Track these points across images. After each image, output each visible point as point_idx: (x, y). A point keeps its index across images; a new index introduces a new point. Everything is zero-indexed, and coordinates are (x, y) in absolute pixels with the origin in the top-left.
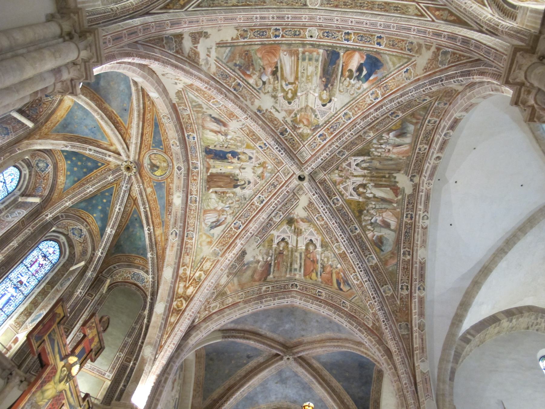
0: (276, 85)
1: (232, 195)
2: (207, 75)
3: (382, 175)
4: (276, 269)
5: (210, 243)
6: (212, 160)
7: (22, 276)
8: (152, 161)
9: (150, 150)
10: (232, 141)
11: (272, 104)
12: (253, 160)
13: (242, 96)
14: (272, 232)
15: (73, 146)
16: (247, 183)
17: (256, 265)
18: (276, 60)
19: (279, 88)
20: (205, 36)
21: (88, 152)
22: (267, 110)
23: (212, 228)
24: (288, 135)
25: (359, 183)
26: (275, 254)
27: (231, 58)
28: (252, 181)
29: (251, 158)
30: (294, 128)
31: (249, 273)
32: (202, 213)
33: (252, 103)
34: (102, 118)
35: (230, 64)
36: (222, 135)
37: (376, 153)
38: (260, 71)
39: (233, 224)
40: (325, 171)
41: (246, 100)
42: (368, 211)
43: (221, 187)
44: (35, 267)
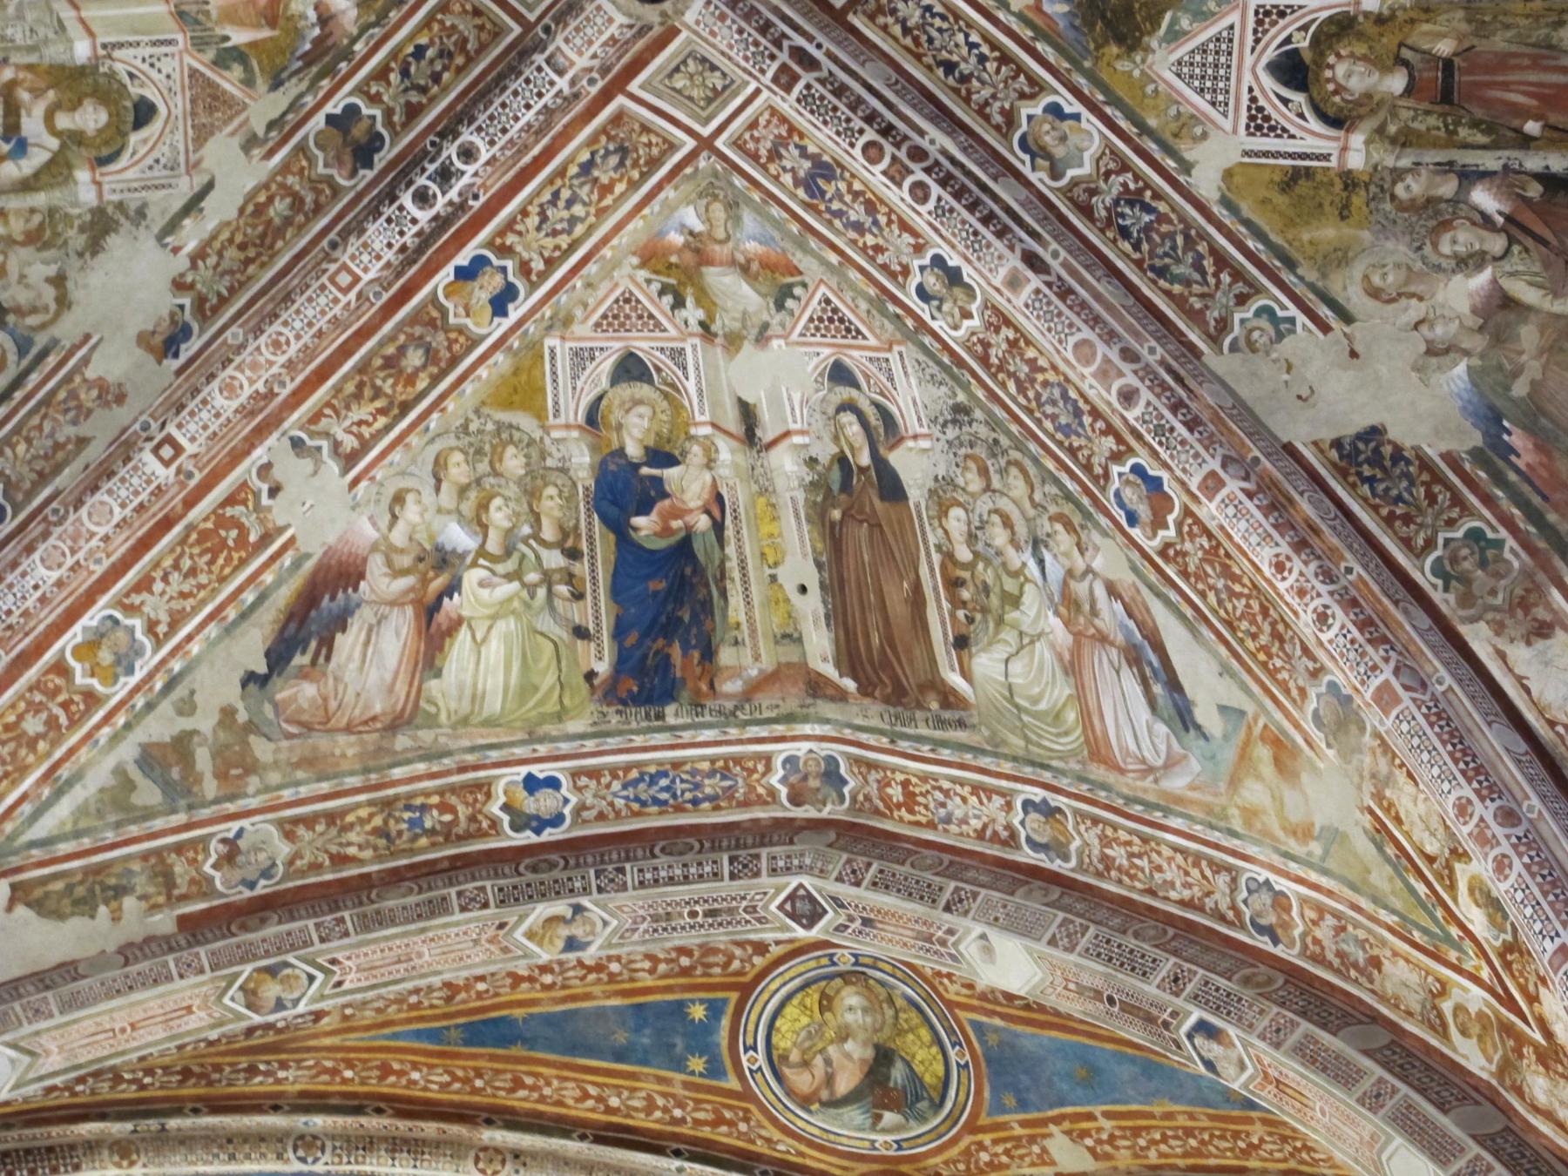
1: (956, 520)
5: (1284, 755)
6: (726, 656)
8: (844, 1085)
9: (747, 1095)
10: (499, 516)
11: (148, 242)
12: (644, 345)
13: (43, 478)
14: (1206, 184)
16: (845, 393)
17: (1528, 335)
19: (40, 199)
22: (179, 285)
23: (1183, 718)
24: (375, 99)
26: (1452, 142)
29: (630, 369)
32: (1111, 778)
33: (113, 395)
36: (453, 588)
39: (1136, 533)
41: (82, 442)
43: (917, 600)
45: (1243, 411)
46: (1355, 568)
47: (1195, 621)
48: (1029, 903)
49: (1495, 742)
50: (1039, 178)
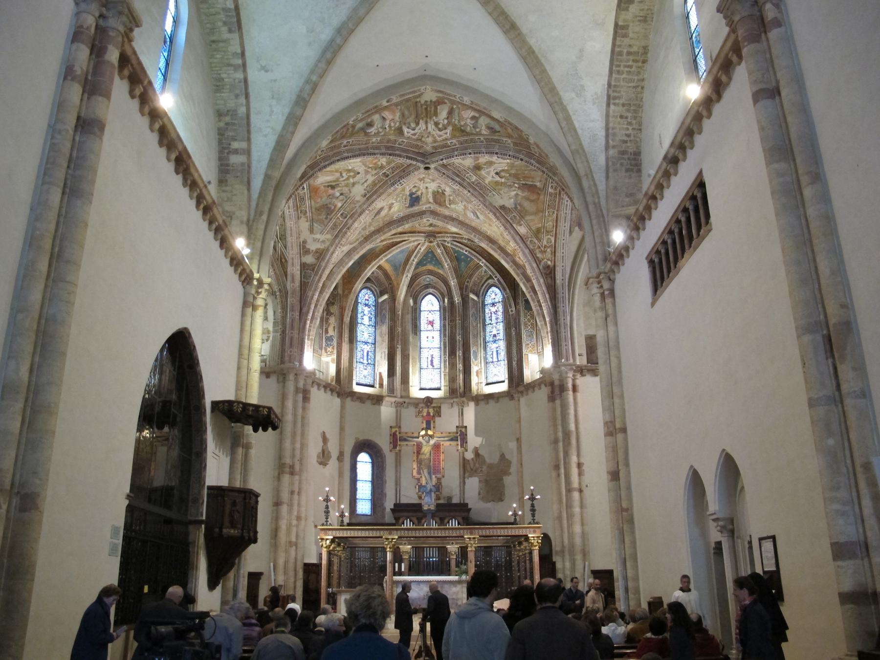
0: (343, 185)
2: (331, 245)
3: (424, 111)
4: (531, 180)
7: (491, 332)
12: (416, 185)
13: (352, 211)
14: (487, 182)
15: (408, 271)
17: (520, 197)
18: (322, 187)
19: (346, 182)
20: (305, 243)
21: (415, 263)
22: (365, 190)
23: (478, 217)
25: (433, 127)
27: (321, 222)
28: (438, 185)
30: (382, 167)
31: (527, 205)
33: (358, 202)
34: (386, 256)
35: (326, 222)
37: (398, 124)
38: (331, 199)
40: (423, 146)
42: (461, 126)
43: (445, 201)
45: (491, 204)
46: (503, 221)
47: (481, 214)
48: (456, 223)
49: (518, 238)
50: (468, 180)
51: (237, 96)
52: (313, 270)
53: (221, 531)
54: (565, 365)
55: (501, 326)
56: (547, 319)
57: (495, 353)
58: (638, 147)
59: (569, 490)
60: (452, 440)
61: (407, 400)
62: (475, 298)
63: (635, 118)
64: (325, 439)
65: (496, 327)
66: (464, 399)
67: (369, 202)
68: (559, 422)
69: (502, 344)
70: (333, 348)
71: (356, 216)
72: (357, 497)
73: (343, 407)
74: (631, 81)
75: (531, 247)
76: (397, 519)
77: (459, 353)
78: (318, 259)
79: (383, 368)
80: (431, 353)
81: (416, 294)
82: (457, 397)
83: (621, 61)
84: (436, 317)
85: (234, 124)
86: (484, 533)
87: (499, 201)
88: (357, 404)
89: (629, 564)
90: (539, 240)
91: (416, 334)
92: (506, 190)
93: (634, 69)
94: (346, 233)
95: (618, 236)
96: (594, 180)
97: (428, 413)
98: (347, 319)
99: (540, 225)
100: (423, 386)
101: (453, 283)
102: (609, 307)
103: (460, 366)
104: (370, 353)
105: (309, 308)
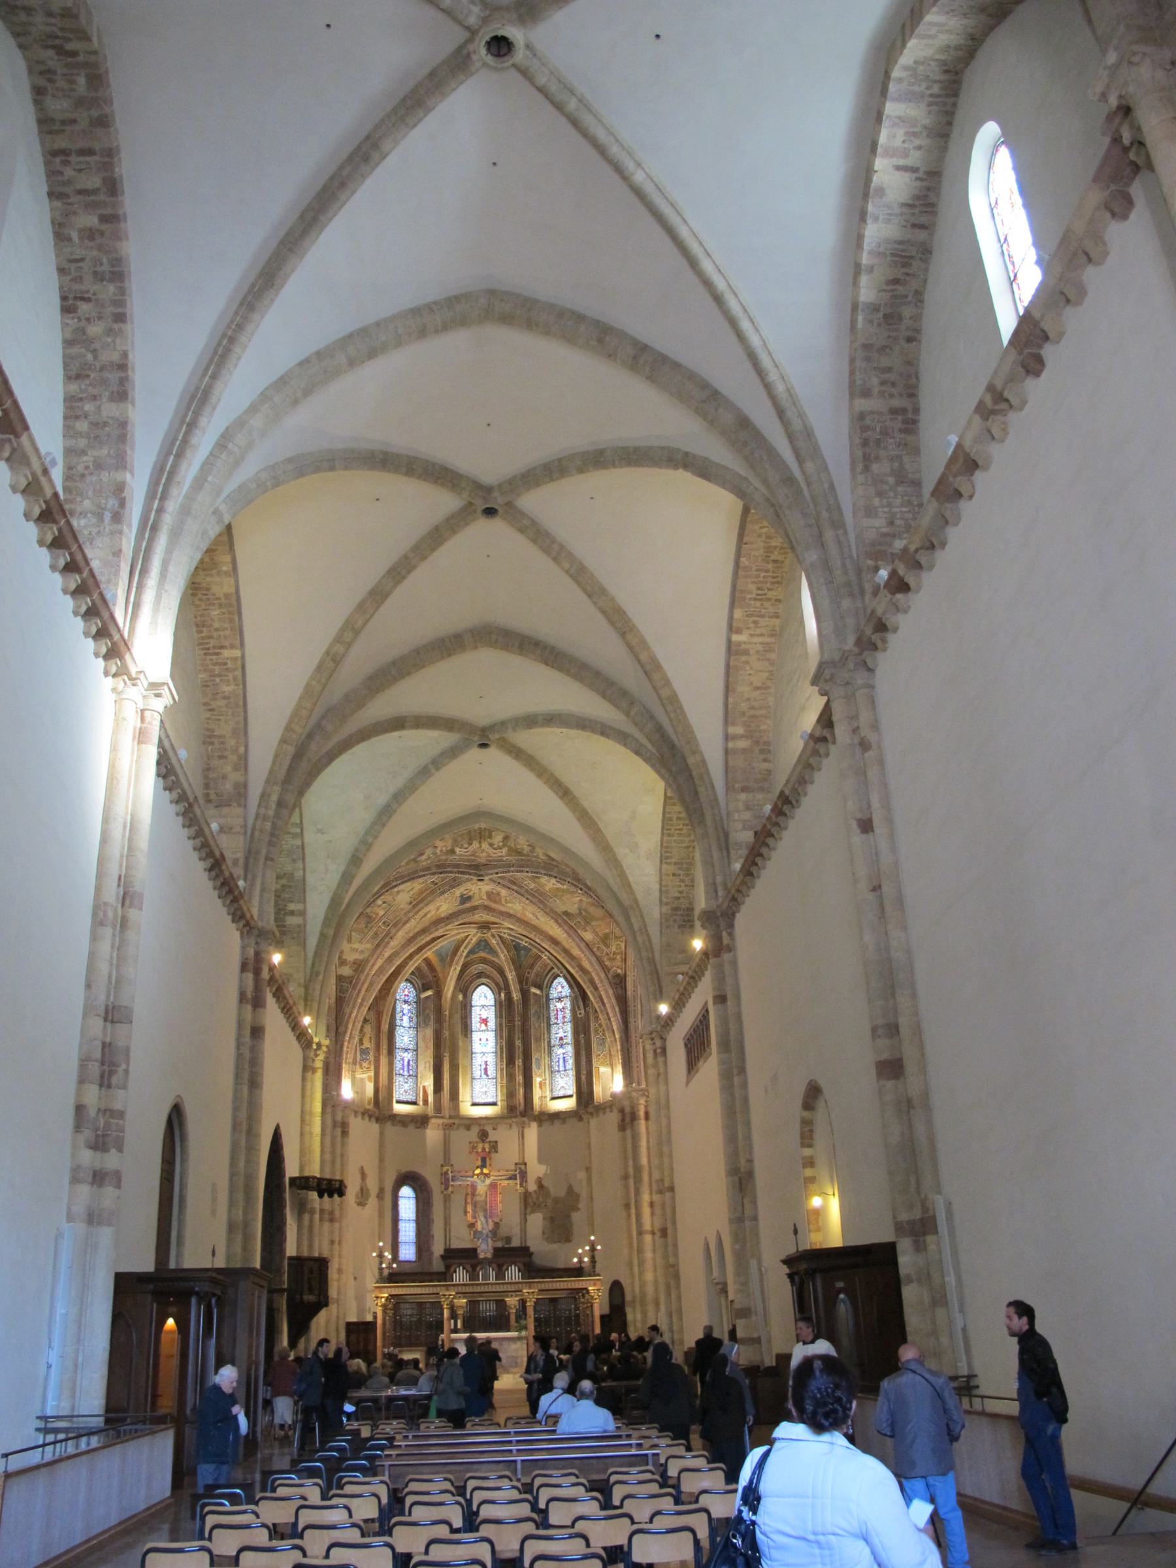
2: (372, 955)
15: (457, 964)
31: (591, 909)
44: (560, 1016)
45: (552, 910)
46: (566, 928)
49: (583, 945)
51: (294, 861)
52: (351, 983)
53: (302, 1298)
54: (635, 1091)
55: (569, 1027)
56: (617, 1036)
57: (561, 1061)
58: (691, 904)
59: (640, 1233)
60: (510, 1178)
61: (456, 1122)
62: (538, 992)
63: (688, 875)
64: (363, 1175)
65: (563, 1030)
66: (525, 1119)
67: (415, 910)
68: (630, 1155)
69: (570, 1049)
70: (370, 1063)
71: (401, 924)
72: (400, 1240)
73: (382, 1133)
74: (683, 842)
75: (598, 954)
76: (448, 1267)
77: (519, 1062)
78: (356, 971)
79: (429, 1083)
80: (484, 1059)
81: (466, 988)
82: (516, 1117)
83: (672, 825)
84: (490, 1014)
85: (290, 887)
86: (543, 1286)
87: (560, 907)
88: (399, 1129)
89: (675, 1318)
90: (607, 946)
91: (466, 1036)
92: (569, 896)
93: (684, 831)
94: (389, 943)
95: (664, 1009)
96: (648, 935)
97: (484, 1149)
98: (385, 1027)
99: (608, 931)
100: (477, 1100)
101: (511, 976)
102: (661, 1064)
103: (520, 1078)
104: (411, 1063)
105: (347, 1028)
